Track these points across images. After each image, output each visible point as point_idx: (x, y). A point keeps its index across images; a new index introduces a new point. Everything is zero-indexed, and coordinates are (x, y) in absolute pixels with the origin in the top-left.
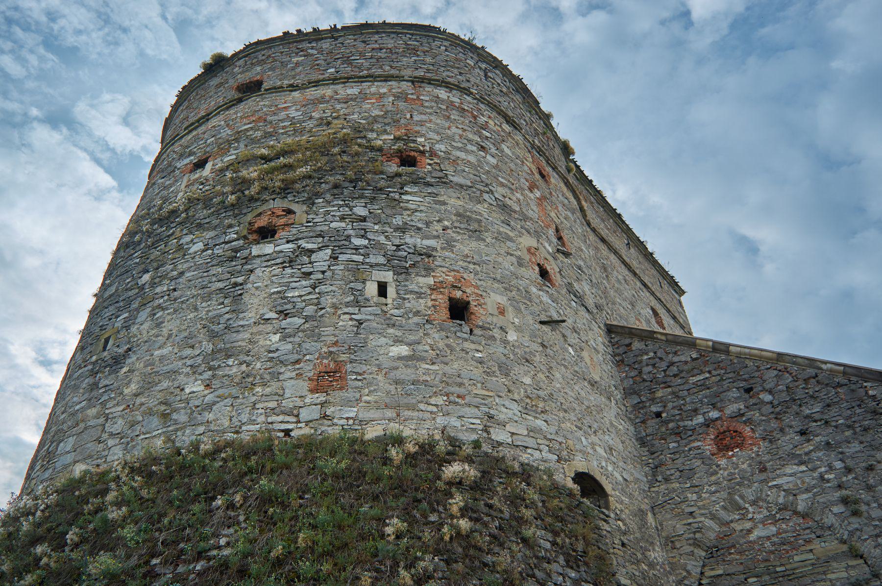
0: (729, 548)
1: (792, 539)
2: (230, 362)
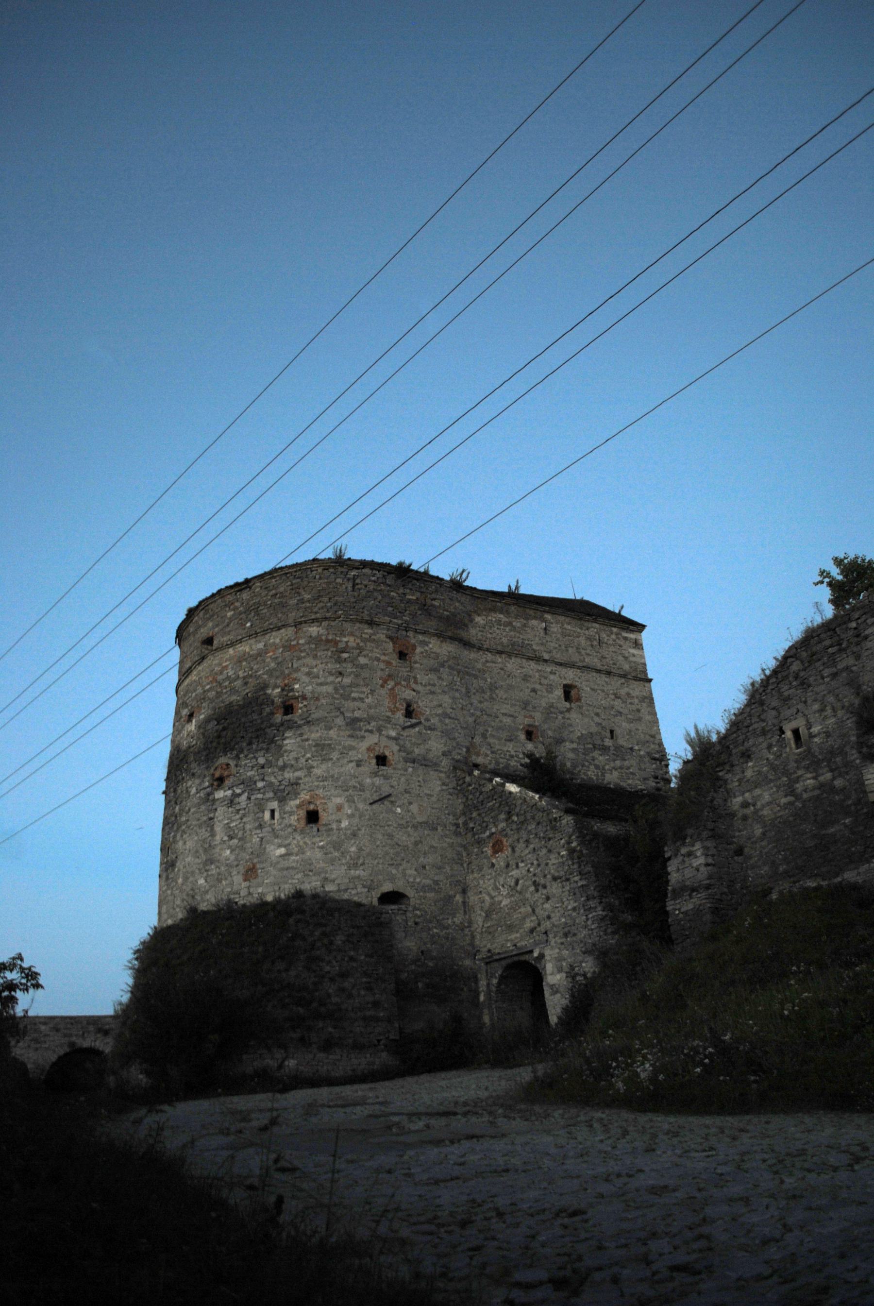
2: (213, 867)
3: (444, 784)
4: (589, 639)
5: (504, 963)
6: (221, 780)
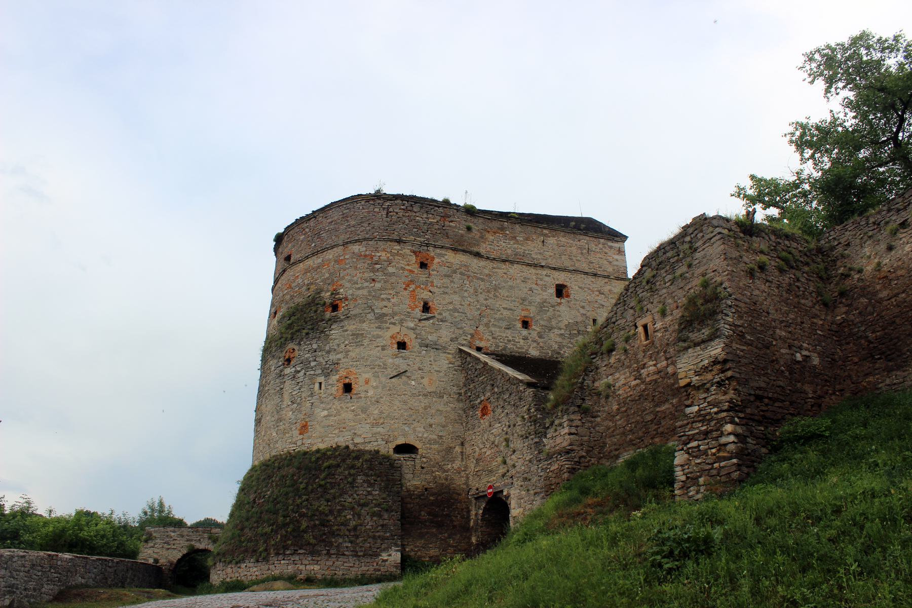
3: (450, 363)
4: (581, 248)
6: (289, 361)
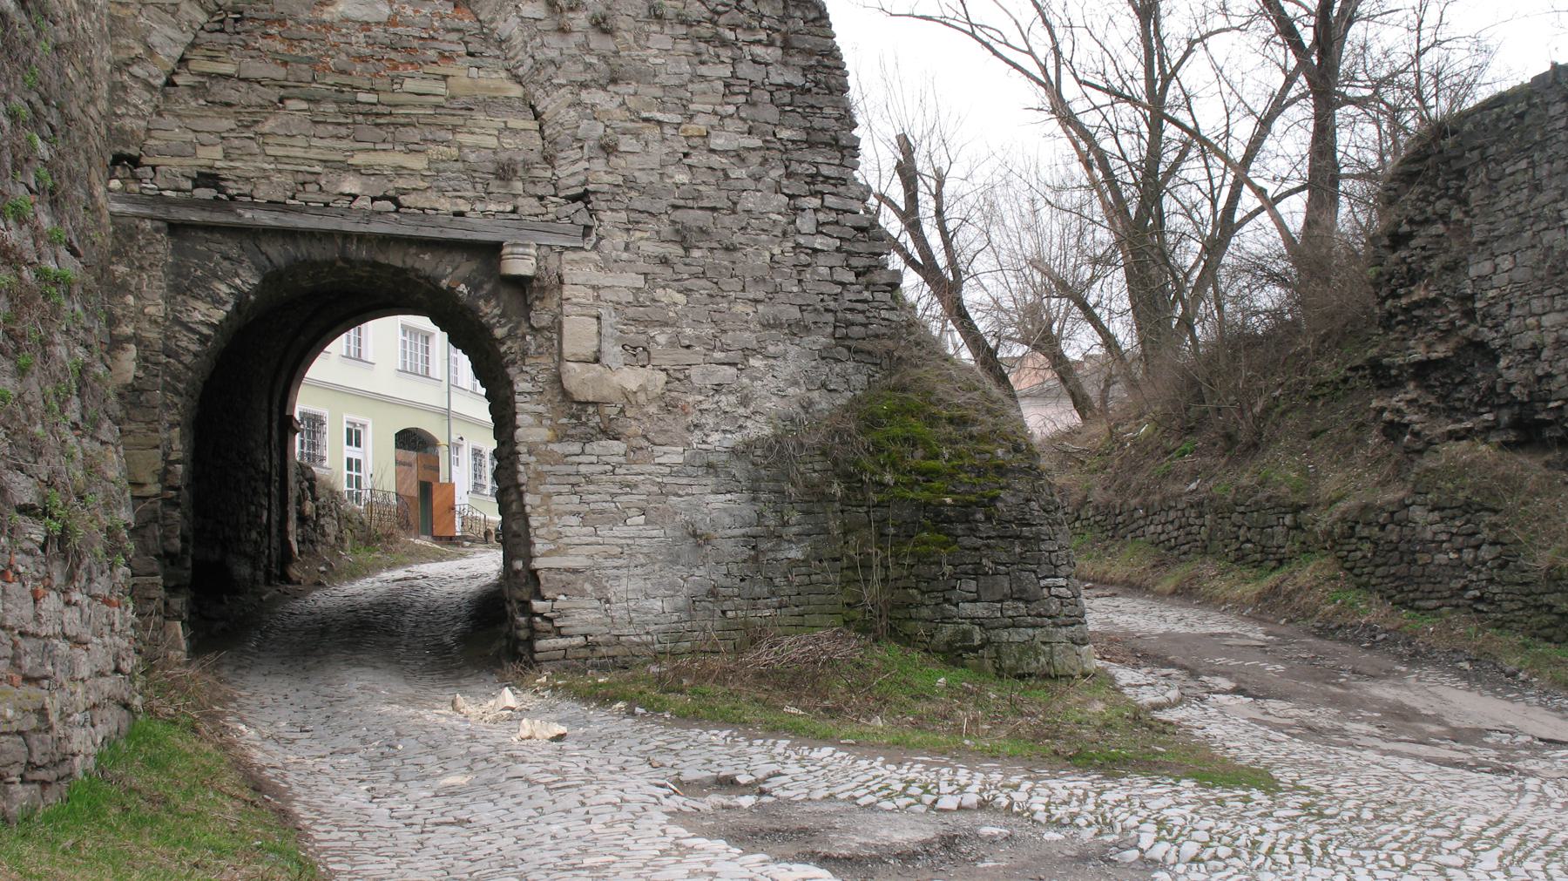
0: (268, 22)
1: (416, 44)
5: (277, 253)
